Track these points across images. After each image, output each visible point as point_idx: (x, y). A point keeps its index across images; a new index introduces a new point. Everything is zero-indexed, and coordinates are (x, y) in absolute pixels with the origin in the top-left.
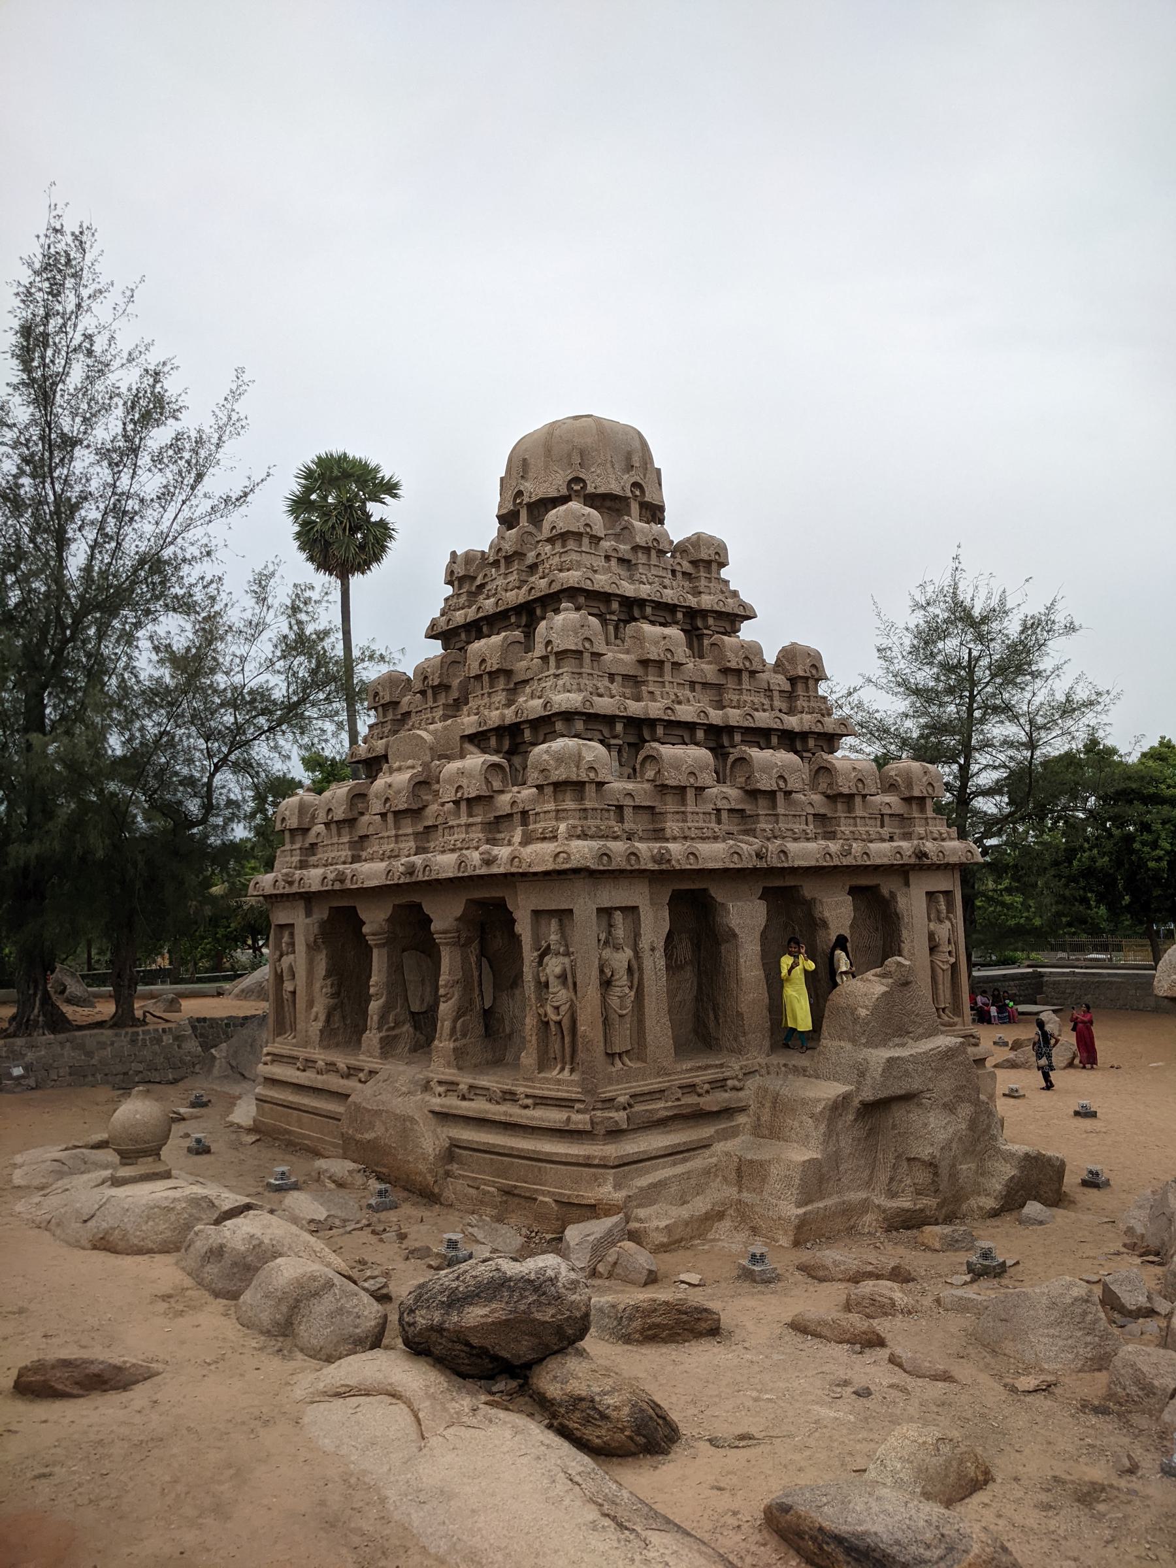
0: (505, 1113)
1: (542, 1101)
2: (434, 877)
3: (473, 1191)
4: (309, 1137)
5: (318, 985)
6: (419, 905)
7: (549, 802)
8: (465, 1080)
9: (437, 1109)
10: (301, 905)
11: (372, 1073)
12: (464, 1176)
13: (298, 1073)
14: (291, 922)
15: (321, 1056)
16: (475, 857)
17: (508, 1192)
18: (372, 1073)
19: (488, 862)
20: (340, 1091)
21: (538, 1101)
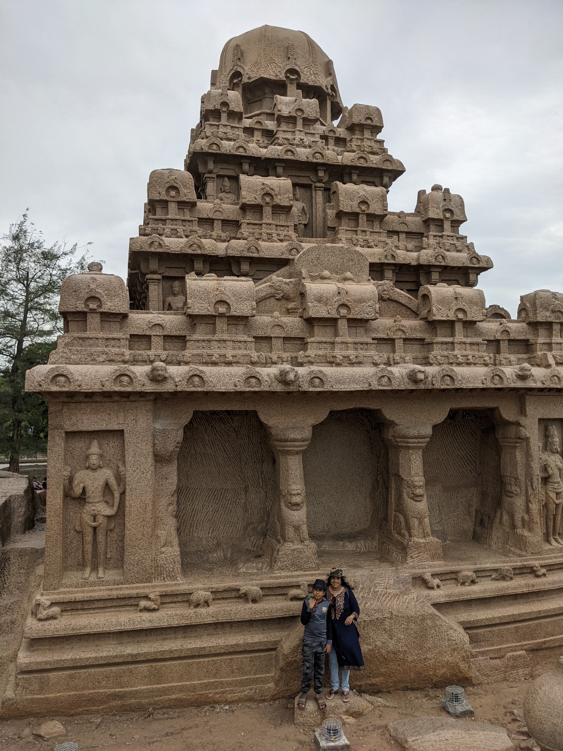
0: (527, 585)
1: (551, 568)
2: (457, 385)
3: (498, 662)
4: (181, 689)
5: (164, 501)
6: (254, 414)
7: (556, 336)
8: (467, 569)
9: (443, 600)
10: (149, 406)
12: (483, 653)
13: (146, 616)
14: (116, 427)
15: (200, 586)
16: (509, 371)
17: (533, 650)
19: (522, 378)
21: (548, 568)
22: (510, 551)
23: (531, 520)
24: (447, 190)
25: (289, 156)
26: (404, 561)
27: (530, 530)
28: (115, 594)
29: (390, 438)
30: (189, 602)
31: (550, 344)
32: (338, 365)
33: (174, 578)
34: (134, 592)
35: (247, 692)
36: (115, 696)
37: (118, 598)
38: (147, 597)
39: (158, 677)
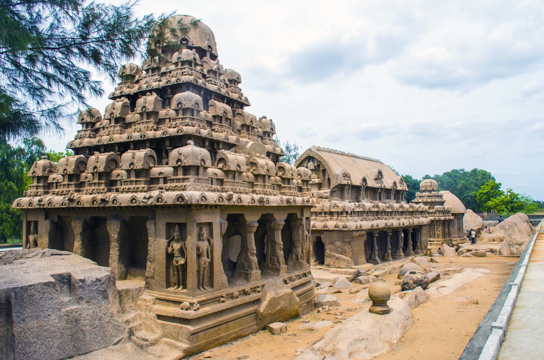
4: (233, 333)
11: (263, 286)
13: (223, 304)
15: (235, 290)
18: (263, 286)
20: (252, 300)
22: (297, 269)
23: (304, 256)
24: (271, 120)
25: (219, 92)
26: (278, 274)
27: (303, 260)
28: (214, 296)
29: (272, 225)
30: (232, 298)
31: (308, 189)
32: (268, 195)
33: (226, 287)
34: (218, 295)
35: (250, 330)
36: (217, 340)
37: (215, 298)
38: (222, 297)
39: (227, 329)
